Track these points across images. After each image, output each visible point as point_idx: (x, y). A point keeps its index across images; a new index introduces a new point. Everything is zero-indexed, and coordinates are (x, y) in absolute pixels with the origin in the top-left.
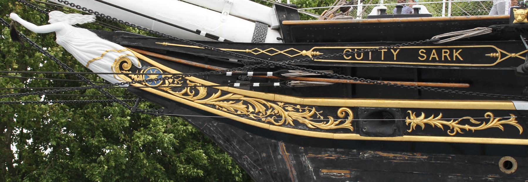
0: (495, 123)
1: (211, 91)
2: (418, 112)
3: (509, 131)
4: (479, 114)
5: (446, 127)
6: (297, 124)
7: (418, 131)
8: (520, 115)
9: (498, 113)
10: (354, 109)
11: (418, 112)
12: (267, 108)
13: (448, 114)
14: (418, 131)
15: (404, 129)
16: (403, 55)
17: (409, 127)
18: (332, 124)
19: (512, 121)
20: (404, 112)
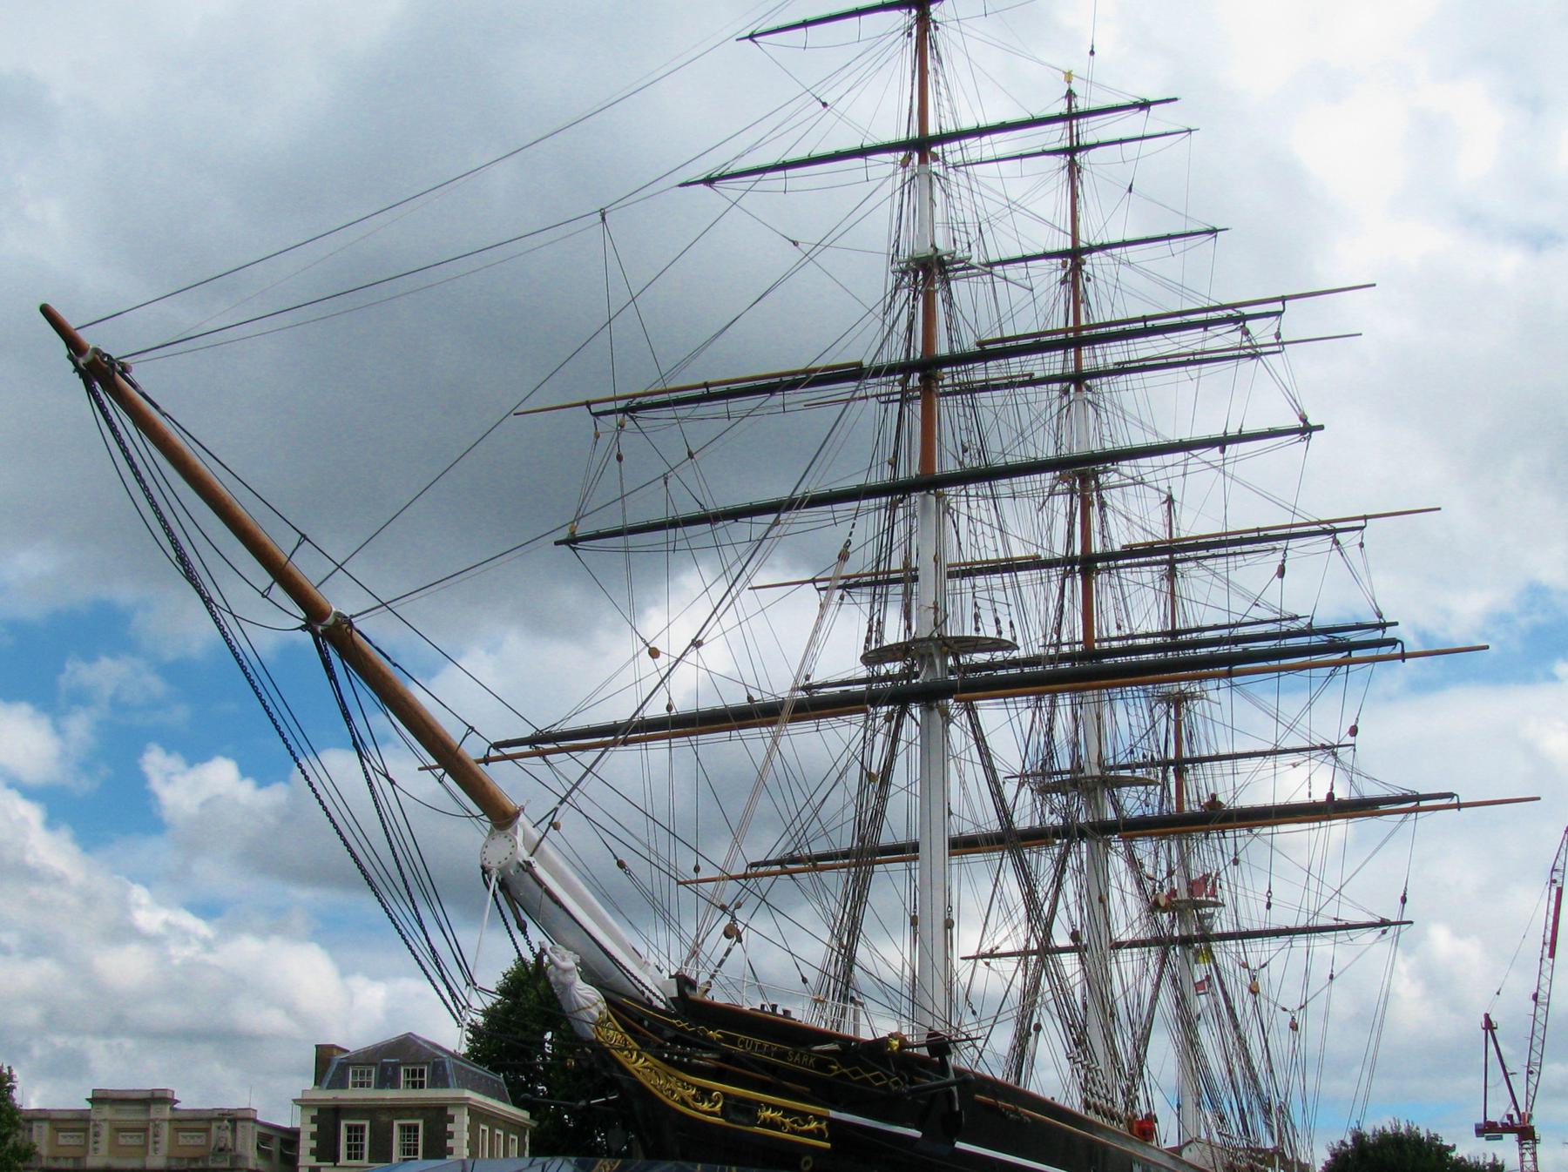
0: (813, 1125)
1: (639, 1056)
2: (768, 1106)
3: (818, 1135)
4: (804, 1116)
5: (783, 1124)
6: (683, 1102)
7: (764, 1124)
8: (832, 1123)
9: (819, 1118)
10: (726, 1095)
11: (768, 1106)
12: (668, 1081)
13: (788, 1112)
14: (764, 1124)
15: (754, 1120)
16: (782, 1055)
17: (758, 1118)
18: (706, 1106)
19: (824, 1125)
20: (758, 1103)
